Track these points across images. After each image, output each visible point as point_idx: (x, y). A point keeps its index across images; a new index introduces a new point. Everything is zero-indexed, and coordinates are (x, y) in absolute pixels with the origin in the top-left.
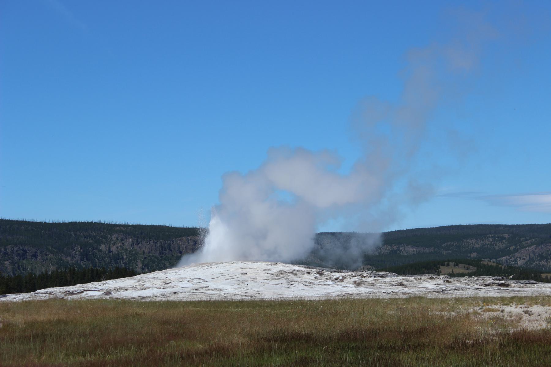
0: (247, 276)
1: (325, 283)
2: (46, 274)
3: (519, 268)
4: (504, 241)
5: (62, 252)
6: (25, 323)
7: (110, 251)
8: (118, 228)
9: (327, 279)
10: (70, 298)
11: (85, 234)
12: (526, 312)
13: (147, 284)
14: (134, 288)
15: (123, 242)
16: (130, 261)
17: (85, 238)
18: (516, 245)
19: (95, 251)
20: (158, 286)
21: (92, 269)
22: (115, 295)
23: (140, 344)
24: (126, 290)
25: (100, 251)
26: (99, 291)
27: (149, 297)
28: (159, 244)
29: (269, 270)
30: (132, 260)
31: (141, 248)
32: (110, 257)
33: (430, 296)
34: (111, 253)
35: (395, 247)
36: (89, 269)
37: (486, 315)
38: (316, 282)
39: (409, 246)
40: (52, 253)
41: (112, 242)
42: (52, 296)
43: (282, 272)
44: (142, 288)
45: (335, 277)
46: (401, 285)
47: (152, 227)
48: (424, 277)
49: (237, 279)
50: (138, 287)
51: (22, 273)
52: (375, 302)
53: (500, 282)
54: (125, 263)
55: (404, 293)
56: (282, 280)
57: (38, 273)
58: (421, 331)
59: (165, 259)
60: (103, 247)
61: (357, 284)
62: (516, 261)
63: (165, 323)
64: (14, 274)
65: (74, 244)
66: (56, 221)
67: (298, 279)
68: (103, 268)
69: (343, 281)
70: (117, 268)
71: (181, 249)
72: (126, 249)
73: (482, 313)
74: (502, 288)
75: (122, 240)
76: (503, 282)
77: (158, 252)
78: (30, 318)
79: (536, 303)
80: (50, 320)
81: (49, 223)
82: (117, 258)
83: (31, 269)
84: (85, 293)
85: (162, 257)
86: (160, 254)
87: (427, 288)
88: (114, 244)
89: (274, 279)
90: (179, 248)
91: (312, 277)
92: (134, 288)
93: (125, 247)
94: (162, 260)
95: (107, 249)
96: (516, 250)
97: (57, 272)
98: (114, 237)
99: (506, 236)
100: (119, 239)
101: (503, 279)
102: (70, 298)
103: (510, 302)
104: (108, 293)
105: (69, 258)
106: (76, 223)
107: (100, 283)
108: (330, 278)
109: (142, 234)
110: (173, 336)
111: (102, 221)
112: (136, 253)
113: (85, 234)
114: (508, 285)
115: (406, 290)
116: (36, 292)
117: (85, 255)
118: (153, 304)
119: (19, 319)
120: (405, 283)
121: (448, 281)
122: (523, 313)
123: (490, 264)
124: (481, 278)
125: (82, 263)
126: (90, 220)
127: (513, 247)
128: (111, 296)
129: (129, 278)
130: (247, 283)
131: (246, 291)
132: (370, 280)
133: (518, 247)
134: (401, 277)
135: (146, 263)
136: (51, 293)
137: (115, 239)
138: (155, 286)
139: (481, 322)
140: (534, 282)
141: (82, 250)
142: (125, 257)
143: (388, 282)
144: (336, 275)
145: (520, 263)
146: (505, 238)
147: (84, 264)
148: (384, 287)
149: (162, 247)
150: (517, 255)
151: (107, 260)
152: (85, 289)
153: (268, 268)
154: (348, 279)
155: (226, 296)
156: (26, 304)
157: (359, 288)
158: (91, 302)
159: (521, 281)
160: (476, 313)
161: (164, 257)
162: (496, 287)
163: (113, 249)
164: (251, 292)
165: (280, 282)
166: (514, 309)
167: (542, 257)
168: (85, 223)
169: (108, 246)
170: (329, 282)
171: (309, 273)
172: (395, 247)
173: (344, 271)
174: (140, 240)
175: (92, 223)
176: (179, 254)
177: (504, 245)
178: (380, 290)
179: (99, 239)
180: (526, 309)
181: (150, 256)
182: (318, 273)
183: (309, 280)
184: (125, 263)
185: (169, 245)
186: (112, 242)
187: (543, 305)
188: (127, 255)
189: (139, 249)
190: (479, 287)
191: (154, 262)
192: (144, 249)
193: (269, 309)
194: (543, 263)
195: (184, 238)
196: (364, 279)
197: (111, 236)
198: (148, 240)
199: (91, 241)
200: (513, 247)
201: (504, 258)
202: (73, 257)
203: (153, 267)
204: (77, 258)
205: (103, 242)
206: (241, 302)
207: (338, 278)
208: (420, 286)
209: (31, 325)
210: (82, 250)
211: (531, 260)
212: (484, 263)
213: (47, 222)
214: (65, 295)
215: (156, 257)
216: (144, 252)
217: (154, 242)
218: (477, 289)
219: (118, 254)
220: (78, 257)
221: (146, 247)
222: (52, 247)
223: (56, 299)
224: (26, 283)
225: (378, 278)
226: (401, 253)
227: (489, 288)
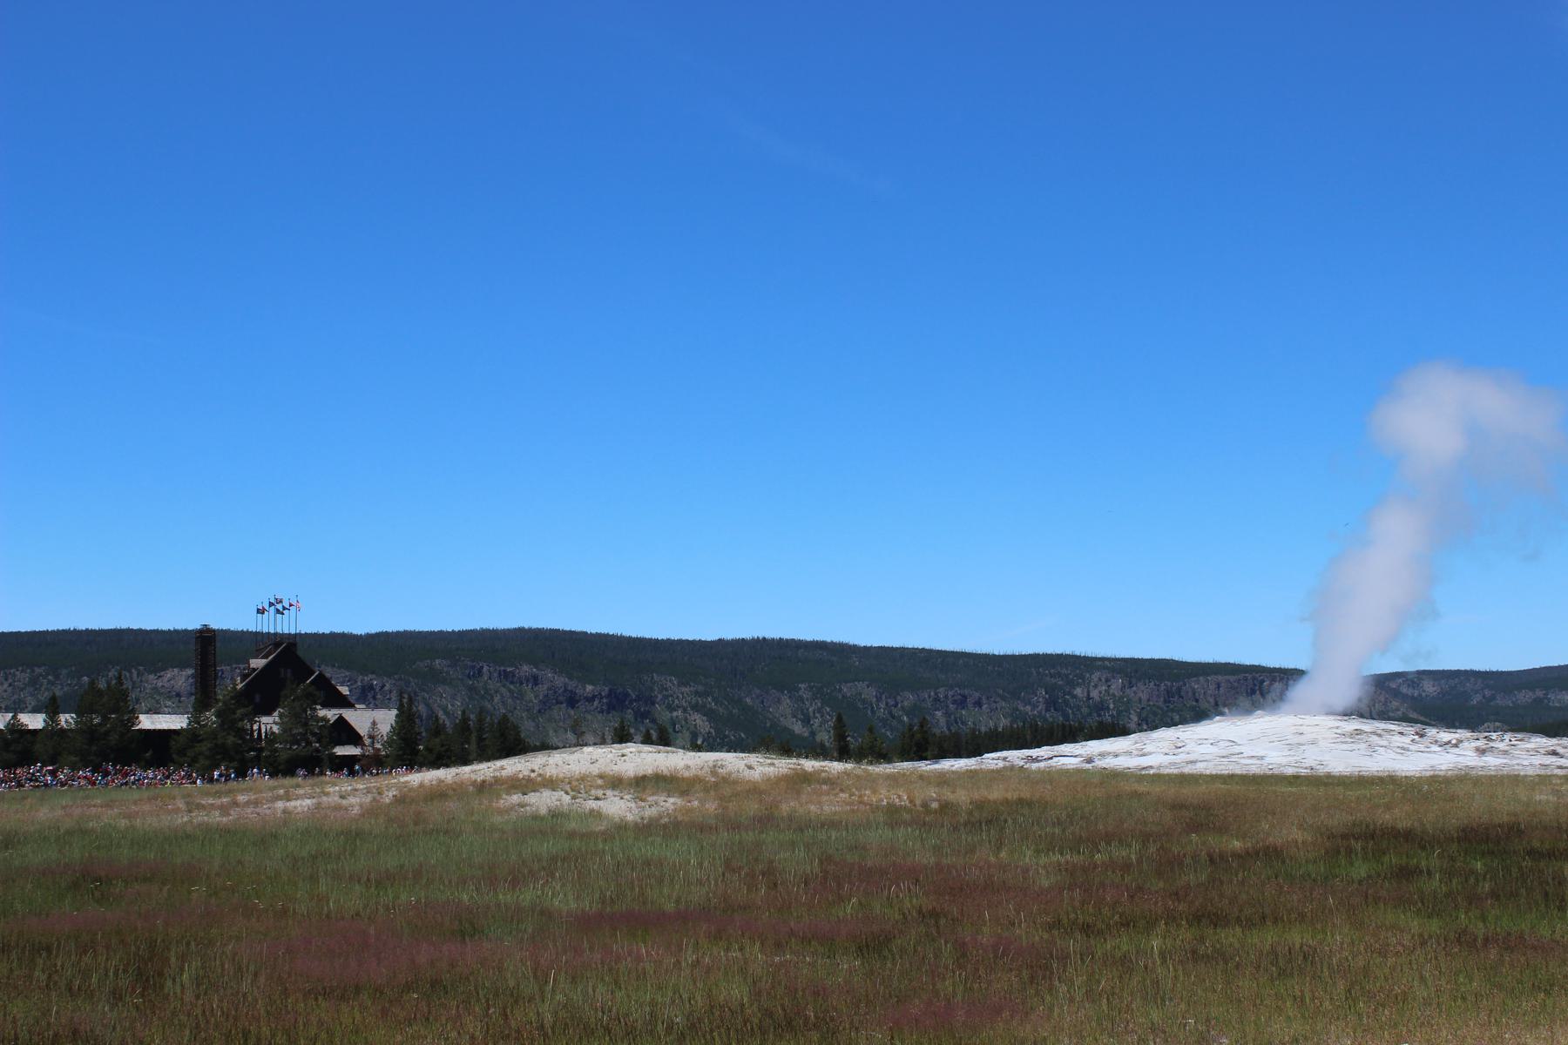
0: (1302, 736)
1: (1428, 750)
5: (1019, 698)
6: (970, 803)
7: (1089, 698)
9: (1431, 743)
10: (1035, 766)
13: (1148, 748)
14: (1129, 753)
15: (1109, 684)
16: (1119, 713)
17: (1051, 677)
19: (1067, 697)
20: (1167, 751)
21: (1063, 724)
22: (1100, 763)
24: (1116, 756)
25: (1075, 697)
26: (1076, 756)
27: (1151, 767)
28: (1163, 687)
29: (1337, 728)
30: (1122, 711)
31: (1135, 692)
32: (1089, 707)
34: (1091, 701)
35: (1539, 693)
36: (1058, 725)
38: (1412, 747)
39: (1564, 692)
40: (1004, 698)
41: (1093, 684)
43: (1359, 732)
44: (1141, 753)
45: (1446, 740)
46: (1554, 753)
47: (1152, 662)
49: (1288, 742)
50: (1135, 752)
51: (959, 728)
52: (1516, 780)
54: (1112, 716)
55: (1560, 767)
56: (1359, 743)
57: (983, 729)
59: (1172, 710)
60: (1078, 691)
61: (1481, 752)
63: (1178, 806)
64: (949, 729)
65: (1036, 686)
66: (1009, 652)
68: (1080, 723)
69: (1457, 747)
70: (1101, 723)
71: (1197, 694)
72: (1114, 695)
75: (1107, 680)
77: (1162, 699)
78: (976, 796)
80: (1007, 799)
81: (999, 656)
82: (1101, 707)
84: (1055, 759)
85: (1168, 707)
86: (1165, 701)
88: (1096, 686)
89: (1346, 743)
90: (1194, 694)
91: (1407, 740)
92: (1129, 753)
93: (1111, 692)
94: (1167, 711)
95: (1086, 694)
97: (1011, 727)
98: (1096, 676)
100: (1103, 680)
102: (1035, 766)
104: (1090, 760)
105: (1028, 708)
106: (1039, 654)
107: (1078, 745)
108: (1436, 741)
109: (1136, 671)
112: (1129, 701)
113: (1052, 671)
116: (983, 757)
117: (1051, 704)
118: (1158, 778)
119: (962, 797)
120: (1560, 750)
125: (1048, 715)
126: (1059, 651)
128: (1093, 764)
129: (1121, 739)
130: (1303, 747)
131: (1303, 761)
132: (1501, 746)
134: (1554, 741)
135: (1144, 715)
136: (1005, 759)
137: (1096, 679)
138: (1158, 750)
141: (1047, 696)
142: (1112, 706)
143: (1533, 749)
144: (1445, 736)
147: (1050, 717)
148: (1525, 757)
149: (1168, 692)
151: (1085, 710)
152: (1056, 753)
153: (1337, 725)
154: (1466, 744)
155: (1270, 767)
156: (972, 774)
157: (1484, 758)
158: (1065, 773)
161: (1172, 706)
163: (1095, 694)
164: (1310, 762)
168: (1051, 655)
169: (1086, 690)
170: (1435, 748)
171: (1401, 733)
172: (1539, 693)
173: (1459, 731)
174: (1134, 681)
176: (1194, 703)
178: (1517, 762)
179: (1073, 679)
181: (1149, 705)
182: (1417, 734)
183: (1403, 745)
184: (1112, 716)
185: (1179, 689)
186: (1093, 684)
188: (1114, 704)
189: (1133, 694)
191: (1155, 714)
192: (1141, 694)
193: (1340, 789)
195: (1201, 678)
196: (1492, 744)
197: (1091, 675)
198: (1147, 681)
202: (1034, 706)
203: (1154, 722)
204: (1040, 708)
205: (1078, 684)
207: (1449, 742)
209: (980, 805)
210: (1047, 696)
213: (997, 653)
214: (1026, 763)
215: (1158, 707)
216: (1140, 700)
217: (1155, 685)
219: (1102, 702)
220: (1041, 707)
221: (1142, 692)
222: (1004, 691)
223: (1012, 768)
224: (967, 743)
225: (1516, 742)
226: (1551, 704)
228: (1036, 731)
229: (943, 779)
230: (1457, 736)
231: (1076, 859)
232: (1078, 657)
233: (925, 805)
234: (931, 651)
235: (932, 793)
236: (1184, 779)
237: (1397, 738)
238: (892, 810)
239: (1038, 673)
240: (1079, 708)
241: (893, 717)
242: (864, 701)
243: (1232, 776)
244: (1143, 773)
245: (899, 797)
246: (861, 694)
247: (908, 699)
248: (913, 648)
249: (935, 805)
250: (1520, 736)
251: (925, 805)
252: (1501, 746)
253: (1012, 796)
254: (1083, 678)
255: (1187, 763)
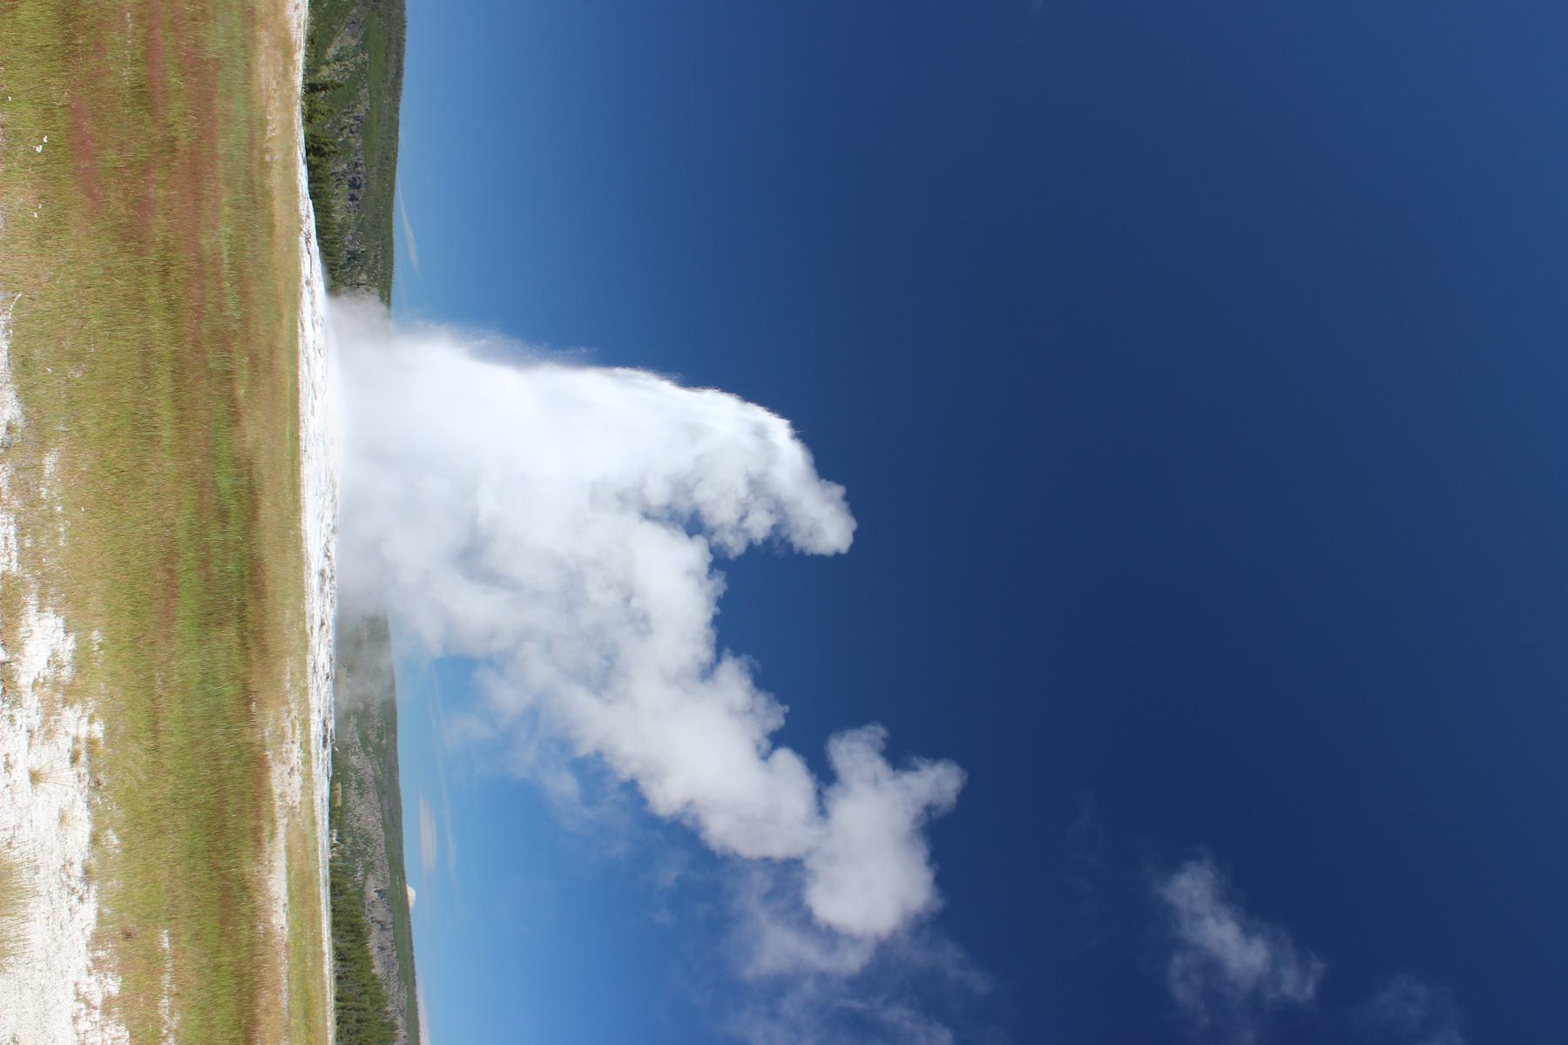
2: (332, 211)
3: (347, 757)
4: (378, 740)
5: (358, 230)
8: (386, 294)
10: (302, 239)
11: (379, 257)
12: (292, 769)
13: (318, 328)
14: (314, 313)
18: (374, 753)
20: (317, 343)
22: (306, 291)
23: (245, 321)
24: (312, 304)
25: (359, 274)
26: (311, 272)
27: (303, 330)
33: (309, 657)
37: (288, 724)
38: (323, 525)
42: (304, 218)
43: (334, 486)
45: (330, 548)
46: (322, 624)
48: (331, 651)
50: (315, 319)
51: (333, 182)
52: (300, 595)
53: (328, 738)
55: (312, 628)
57: (333, 201)
58: (264, 650)
60: (364, 277)
61: (322, 574)
62: (355, 754)
63: (272, 350)
64: (332, 174)
67: (326, 504)
73: (290, 719)
74: (321, 741)
76: (329, 741)
78: (276, 193)
79: (304, 780)
83: (337, 194)
84: (308, 256)
87: (318, 655)
89: (326, 477)
96: (367, 753)
99: (384, 742)
101: (332, 740)
103: (304, 751)
104: (308, 283)
105: (351, 237)
106: (392, 246)
108: (328, 542)
110: (254, 359)
111: (394, 277)
113: (379, 257)
114: (325, 746)
115: (316, 630)
117: (353, 256)
118: (294, 336)
119: (275, 180)
120: (325, 628)
121: (328, 677)
122: (292, 765)
123: (351, 724)
124: (333, 715)
127: (370, 749)
128: (305, 285)
130: (321, 445)
133: (371, 756)
134: (331, 624)
136: (308, 216)
139: (277, 719)
140: (330, 776)
145: (353, 759)
146: (381, 740)
150: (363, 754)
152: (313, 257)
157: (317, 575)
158: (297, 264)
159: (330, 761)
160: (289, 712)
162: (322, 734)
165: (323, 482)
166: (296, 755)
167: (360, 783)
168: (393, 256)
170: (324, 541)
171: (334, 516)
175: (392, 264)
177: (373, 740)
180: (296, 769)
182: (334, 528)
187: (302, 788)
190: (322, 714)
193: (289, 471)
194: (354, 785)
196: (328, 581)
199: (371, 263)
200: (370, 749)
201: (358, 741)
202: (351, 242)
206: (297, 439)
207: (328, 551)
208: (321, 645)
209: (268, 194)
211: (357, 771)
212: (352, 717)
213: (394, 214)
218: (319, 711)
220: (351, 248)
223: (301, 222)
224: (321, 188)
227: (321, 725)
228: (332, 243)
229: (289, 166)
230: (333, 557)
231: (226, 267)
232: (391, 277)
233: (267, 150)
234: (395, 162)
235: (278, 157)
236: (294, 354)
237: (331, 514)
238: (264, 124)
239: (378, 246)
240: (351, 277)
241: (342, 129)
242: (354, 106)
243: (297, 391)
244: (299, 324)
245: (274, 129)
246: (360, 104)
247: (357, 143)
248: (397, 147)
249: (267, 158)
250: (335, 600)
251: (267, 150)
252: (327, 588)
253: (277, 219)
254: (375, 280)
255: (308, 358)
